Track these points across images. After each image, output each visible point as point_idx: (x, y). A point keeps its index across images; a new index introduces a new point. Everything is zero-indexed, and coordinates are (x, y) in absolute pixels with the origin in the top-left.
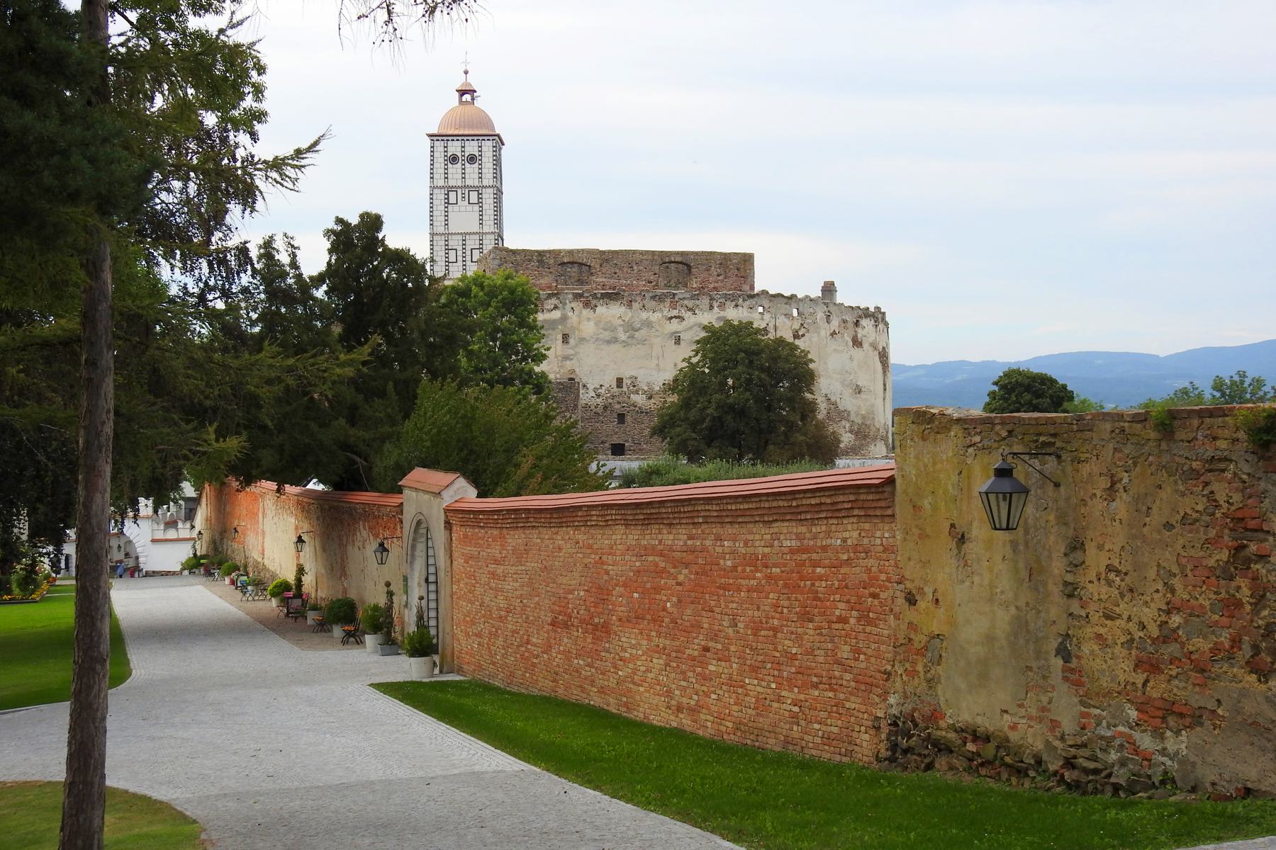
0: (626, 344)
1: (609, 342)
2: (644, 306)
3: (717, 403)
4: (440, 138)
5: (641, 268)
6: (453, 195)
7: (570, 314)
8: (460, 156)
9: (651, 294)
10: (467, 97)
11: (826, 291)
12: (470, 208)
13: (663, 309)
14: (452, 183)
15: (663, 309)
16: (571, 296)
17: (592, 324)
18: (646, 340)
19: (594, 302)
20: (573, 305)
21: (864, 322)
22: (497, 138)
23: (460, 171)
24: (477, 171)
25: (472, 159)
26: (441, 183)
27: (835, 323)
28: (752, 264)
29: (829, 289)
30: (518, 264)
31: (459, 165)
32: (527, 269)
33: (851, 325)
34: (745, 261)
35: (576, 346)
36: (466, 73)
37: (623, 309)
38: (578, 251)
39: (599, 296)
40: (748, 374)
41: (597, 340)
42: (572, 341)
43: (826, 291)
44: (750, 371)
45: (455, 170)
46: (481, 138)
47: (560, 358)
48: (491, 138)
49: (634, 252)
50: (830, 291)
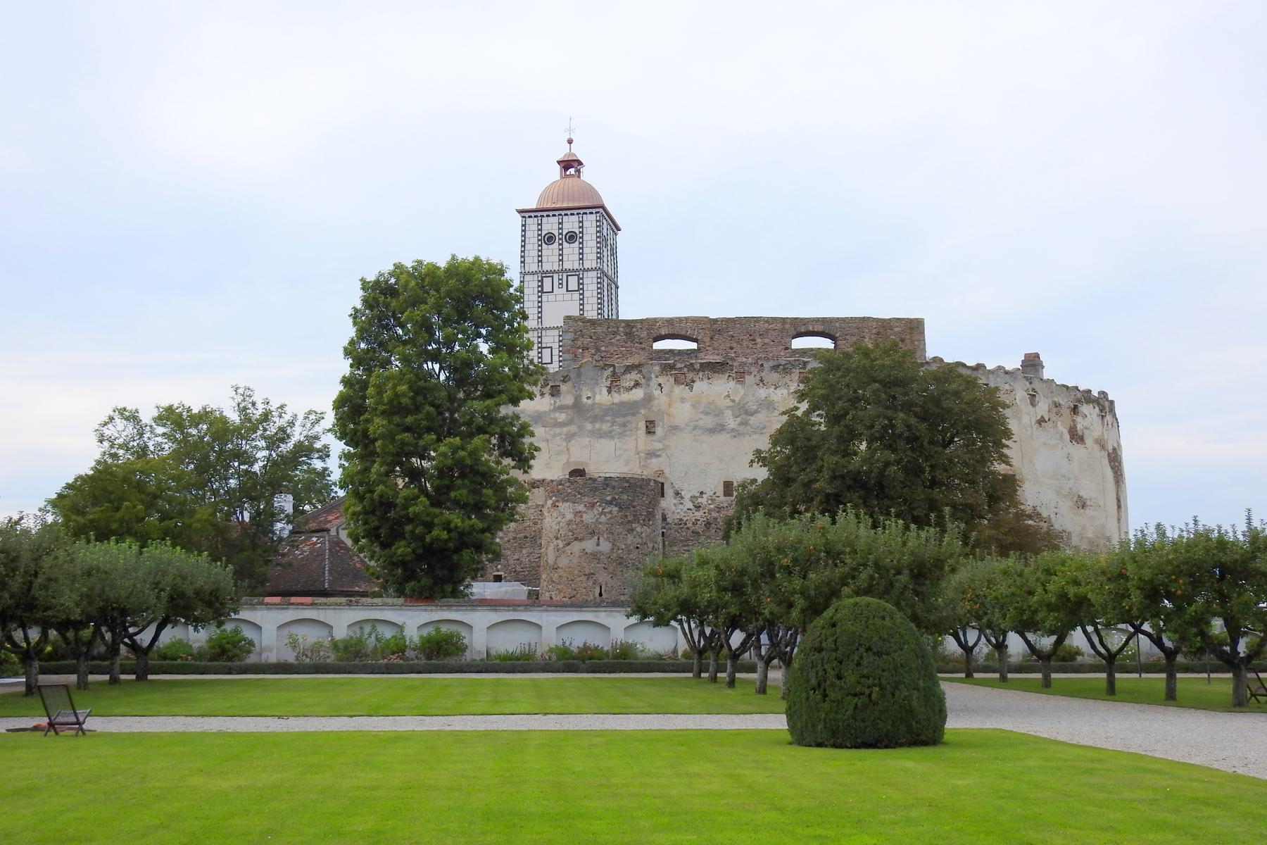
0: (736, 433)
1: (712, 431)
2: (762, 380)
3: (834, 471)
4: (533, 214)
5: (766, 341)
6: (547, 282)
7: (657, 393)
8: (557, 234)
9: (771, 363)
10: (572, 171)
11: (1027, 366)
12: (568, 296)
13: (790, 383)
14: (547, 267)
15: (790, 383)
16: (657, 368)
17: (687, 406)
18: (763, 428)
19: (690, 375)
20: (661, 380)
21: (1085, 409)
22: (601, 210)
23: (556, 252)
24: (577, 251)
25: (571, 237)
26: (534, 268)
27: (1043, 407)
28: (922, 333)
29: (1032, 363)
30: (598, 339)
31: (556, 245)
32: (611, 344)
33: (1066, 412)
34: (912, 329)
35: (665, 437)
36: (570, 142)
37: (732, 384)
38: (680, 320)
39: (698, 366)
40: (887, 418)
41: (695, 428)
42: (659, 431)
43: (1027, 366)
44: (890, 413)
45: (551, 251)
46: (582, 211)
47: (642, 455)
48: (594, 211)
49: (757, 320)
50: (1034, 366)
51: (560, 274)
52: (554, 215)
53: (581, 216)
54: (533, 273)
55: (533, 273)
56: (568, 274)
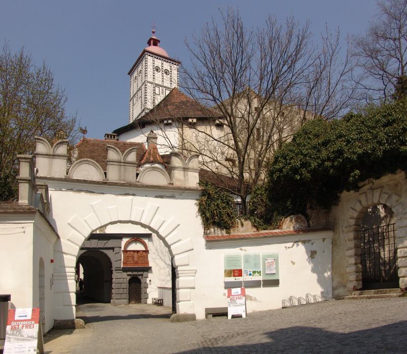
6: (157, 89)
8: (161, 68)
14: (157, 82)
25: (166, 72)
31: (160, 73)
45: (158, 75)
54: (151, 83)
55: (151, 83)
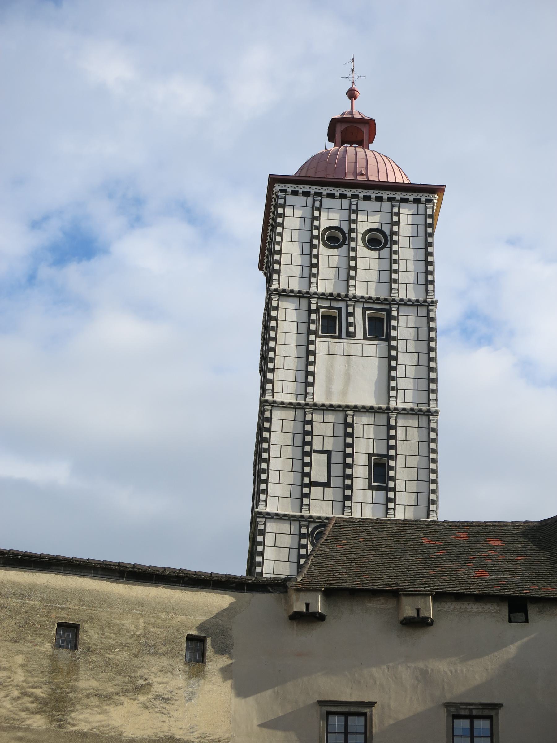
4: (301, 189)
36: (352, 94)
51: (350, 304)
52: (343, 196)
53: (395, 203)
56: (367, 305)
